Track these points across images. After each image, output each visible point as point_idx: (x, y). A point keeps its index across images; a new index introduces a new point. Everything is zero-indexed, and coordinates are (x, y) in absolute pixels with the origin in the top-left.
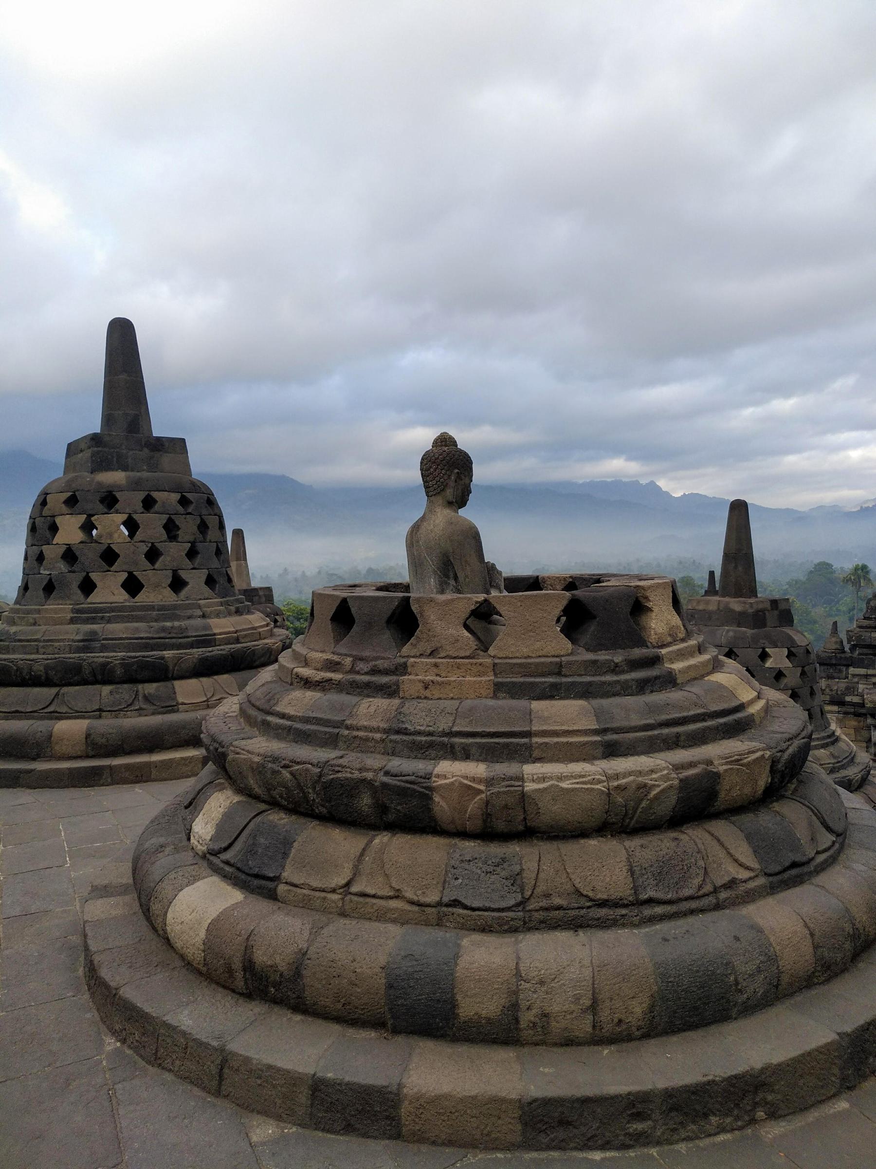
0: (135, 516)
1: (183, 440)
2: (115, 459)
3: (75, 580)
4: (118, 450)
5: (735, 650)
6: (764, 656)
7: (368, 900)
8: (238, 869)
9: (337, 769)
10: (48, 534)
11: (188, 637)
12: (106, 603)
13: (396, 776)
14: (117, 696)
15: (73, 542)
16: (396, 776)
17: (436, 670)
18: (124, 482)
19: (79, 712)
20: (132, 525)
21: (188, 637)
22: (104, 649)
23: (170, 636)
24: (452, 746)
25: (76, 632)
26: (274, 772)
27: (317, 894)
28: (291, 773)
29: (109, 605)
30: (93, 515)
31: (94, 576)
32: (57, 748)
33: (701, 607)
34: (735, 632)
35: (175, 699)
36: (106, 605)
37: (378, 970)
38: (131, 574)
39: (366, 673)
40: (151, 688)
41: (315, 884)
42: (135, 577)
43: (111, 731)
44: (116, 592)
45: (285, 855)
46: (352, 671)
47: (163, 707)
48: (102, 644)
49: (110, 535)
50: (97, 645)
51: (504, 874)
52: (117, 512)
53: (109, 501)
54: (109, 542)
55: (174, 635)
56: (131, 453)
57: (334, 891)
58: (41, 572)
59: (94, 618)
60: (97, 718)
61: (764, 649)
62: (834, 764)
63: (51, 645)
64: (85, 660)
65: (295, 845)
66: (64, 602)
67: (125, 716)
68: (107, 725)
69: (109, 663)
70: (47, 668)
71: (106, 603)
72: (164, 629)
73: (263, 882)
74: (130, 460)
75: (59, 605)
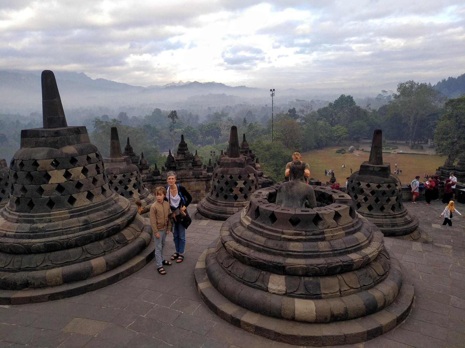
0: (86, 167)
1: (85, 127)
2: (66, 141)
3: (66, 199)
4: (66, 136)
5: (241, 175)
6: (249, 176)
7: (347, 291)
8: (306, 295)
9: (331, 264)
10: (44, 179)
11: (118, 213)
12: (84, 206)
13: (346, 262)
14: (108, 244)
15: (61, 182)
16: (346, 262)
17: (332, 232)
18: (76, 152)
19: (97, 255)
20: (85, 171)
21: (118, 213)
22: (94, 226)
23: (113, 214)
24: (349, 251)
25: (77, 222)
26: (313, 269)
27: (334, 294)
28: (318, 268)
29: (85, 207)
30: (69, 169)
31: (74, 196)
32: (95, 272)
33: (226, 162)
34: (239, 169)
35: (126, 239)
36: (84, 207)
37: (363, 305)
38: (89, 192)
39: (312, 235)
40: (117, 237)
41: (332, 292)
42: (91, 192)
43: (114, 259)
44: (85, 200)
45: (320, 287)
46: (306, 235)
47: (124, 244)
48: (93, 225)
49: (78, 177)
50: (90, 225)
51: (368, 276)
52: (79, 166)
53: (73, 161)
54: (78, 180)
55: (114, 214)
56: (70, 136)
57: (337, 292)
58: (42, 197)
59: (81, 214)
60: (104, 255)
61: (248, 174)
63: (70, 230)
64: (92, 234)
65: (321, 284)
66: (62, 209)
67: (114, 251)
68: (111, 257)
69: (102, 232)
70: (76, 240)
71: (84, 206)
72: (110, 212)
73: (317, 296)
74: (71, 140)
75: (60, 211)
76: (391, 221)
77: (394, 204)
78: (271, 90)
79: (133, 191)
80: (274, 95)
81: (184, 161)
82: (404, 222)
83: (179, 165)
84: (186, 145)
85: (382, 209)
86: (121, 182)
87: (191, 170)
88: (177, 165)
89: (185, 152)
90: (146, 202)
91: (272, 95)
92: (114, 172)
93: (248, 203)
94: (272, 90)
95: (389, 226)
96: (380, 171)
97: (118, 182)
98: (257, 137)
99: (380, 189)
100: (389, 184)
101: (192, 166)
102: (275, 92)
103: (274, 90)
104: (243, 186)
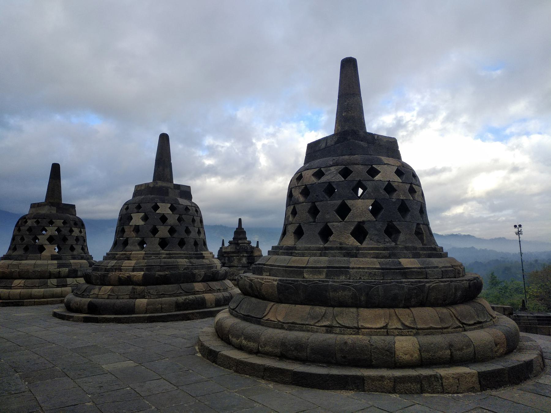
62: (189, 265)
76: (330, 262)
77: (363, 222)
78: (515, 226)
79: (44, 246)
80: (522, 234)
81: (235, 255)
82: (382, 269)
83: (229, 260)
84: (244, 233)
85: (326, 233)
86: (30, 229)
87: (244, 268)
88: (226, 261)
89: (240, 242)
90: (58, 264)
91: (519, 233)
92: (27, 217)
93: (141, 254)
94: (518, 227)
95: (320, 273)
96: (336, 143)
97: (27, 229)
98: (507, 297)
99: (324, 179)
100: (347, 166)
101: (248, 263)
102: (523, 229)
103: (520, 226)
104: (141, 223)
